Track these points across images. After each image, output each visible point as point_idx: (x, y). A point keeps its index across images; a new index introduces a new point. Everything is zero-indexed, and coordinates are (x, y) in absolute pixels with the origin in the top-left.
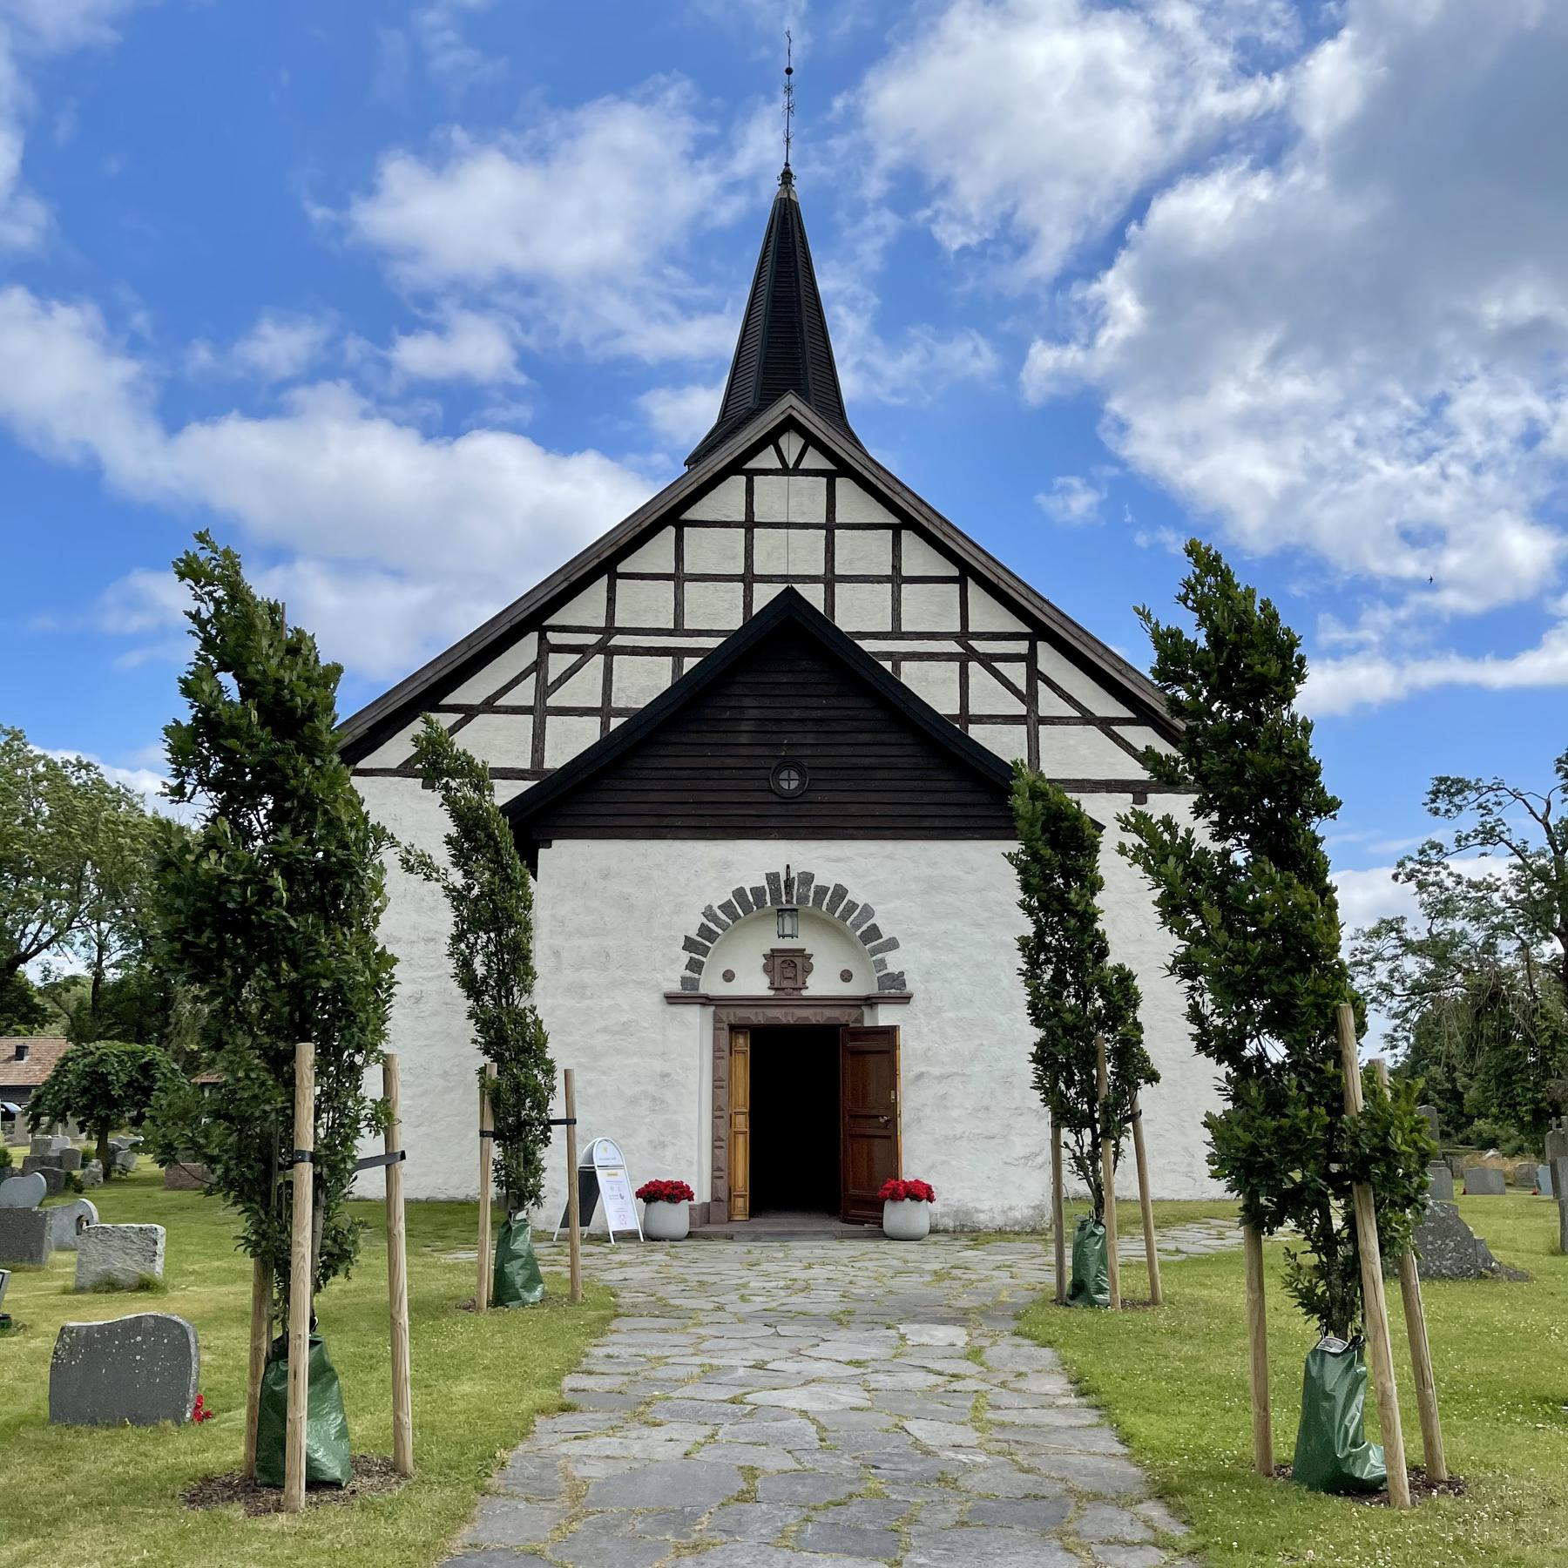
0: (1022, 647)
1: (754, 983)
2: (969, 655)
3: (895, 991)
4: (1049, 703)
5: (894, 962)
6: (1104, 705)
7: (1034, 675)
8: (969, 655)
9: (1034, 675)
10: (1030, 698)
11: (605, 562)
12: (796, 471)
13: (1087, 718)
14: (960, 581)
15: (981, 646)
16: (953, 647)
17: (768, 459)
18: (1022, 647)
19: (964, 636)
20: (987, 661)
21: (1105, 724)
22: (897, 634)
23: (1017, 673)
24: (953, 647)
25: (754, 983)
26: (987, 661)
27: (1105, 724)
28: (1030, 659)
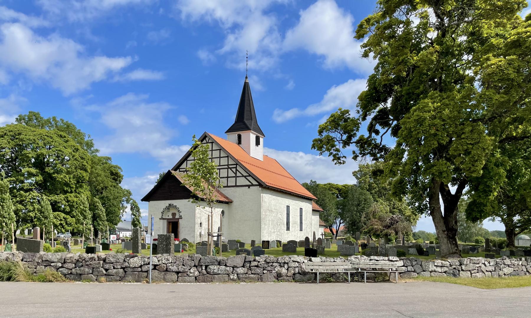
0: (235, 166)
1: (171, 217)
2: (229, 168)
3: (181, 217)
4: (238, 174)
5: (181, 214)
6: (245, 174)
7: (237, 170)
8: (229, 168)
9: (237, 170)
10: (236, 174)
11: (185, 159)
12: (208, 143)
13: (243, 176)
14: (228, 157)
15: (230, 166)
16: (227, 167)
17: (204, 141)
18: (235, 166)
19: (228, 165)
20: (231, 168)
21: (245, 177)
22: (220, 166)
23: (234, 170)
24: (227, 167)
25: (171, 217)
26: (231, 168)
27: (245, 177)
28: (236, 168)
